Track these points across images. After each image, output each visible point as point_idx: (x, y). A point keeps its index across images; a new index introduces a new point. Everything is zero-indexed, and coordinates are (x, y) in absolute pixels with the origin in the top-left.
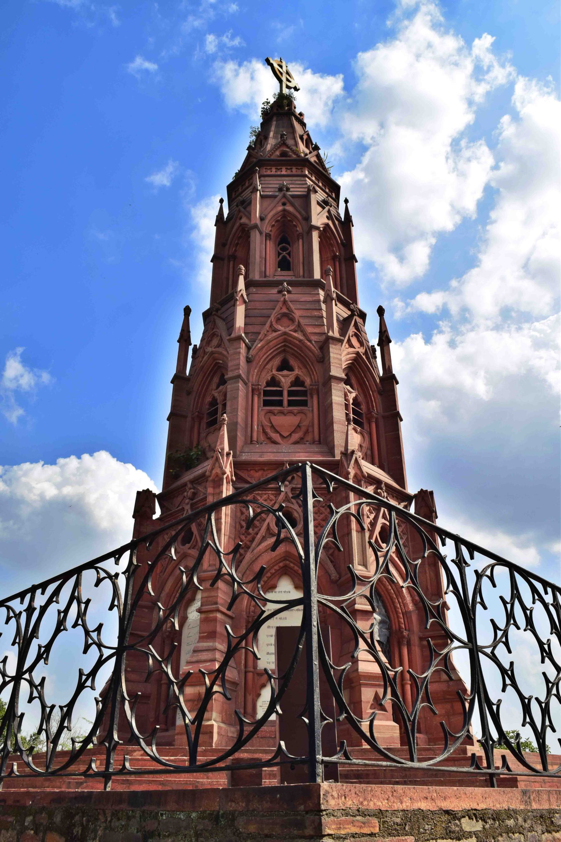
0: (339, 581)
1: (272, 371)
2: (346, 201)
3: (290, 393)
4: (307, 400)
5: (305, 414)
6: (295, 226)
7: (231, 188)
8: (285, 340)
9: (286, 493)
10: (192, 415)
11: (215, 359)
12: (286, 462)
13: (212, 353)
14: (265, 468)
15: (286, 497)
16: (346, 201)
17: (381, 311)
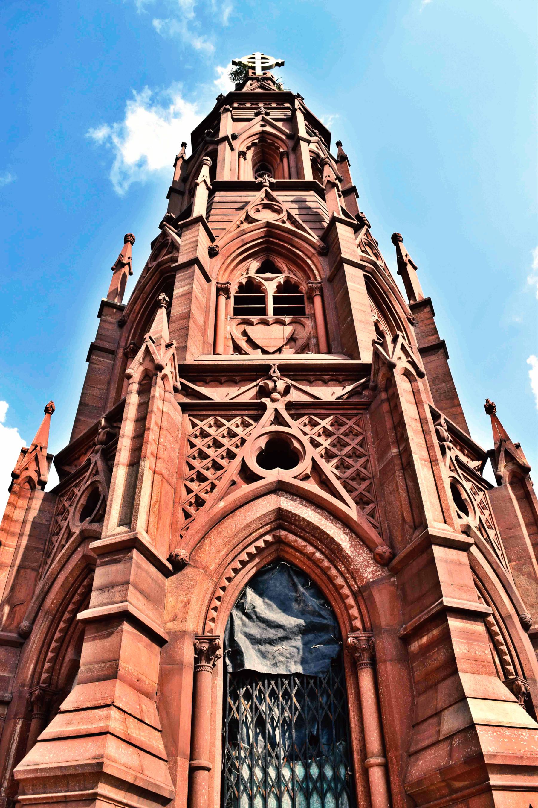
0: (395, 561)
1: (247, 273)
2: (339, 144)
3: (276, 300)
4: (304, 308)
5: (303, 325)
6: (278, 148)
7: (196, 135)
8: (268, 234)
9: (276, 410)
10: (124, 349)
11: (162, 273)
12: (274, 365)
13: (159, 265)
14: (237, 378)
15: (276, 417)
16: (339, 144)
17: (396, 239)
